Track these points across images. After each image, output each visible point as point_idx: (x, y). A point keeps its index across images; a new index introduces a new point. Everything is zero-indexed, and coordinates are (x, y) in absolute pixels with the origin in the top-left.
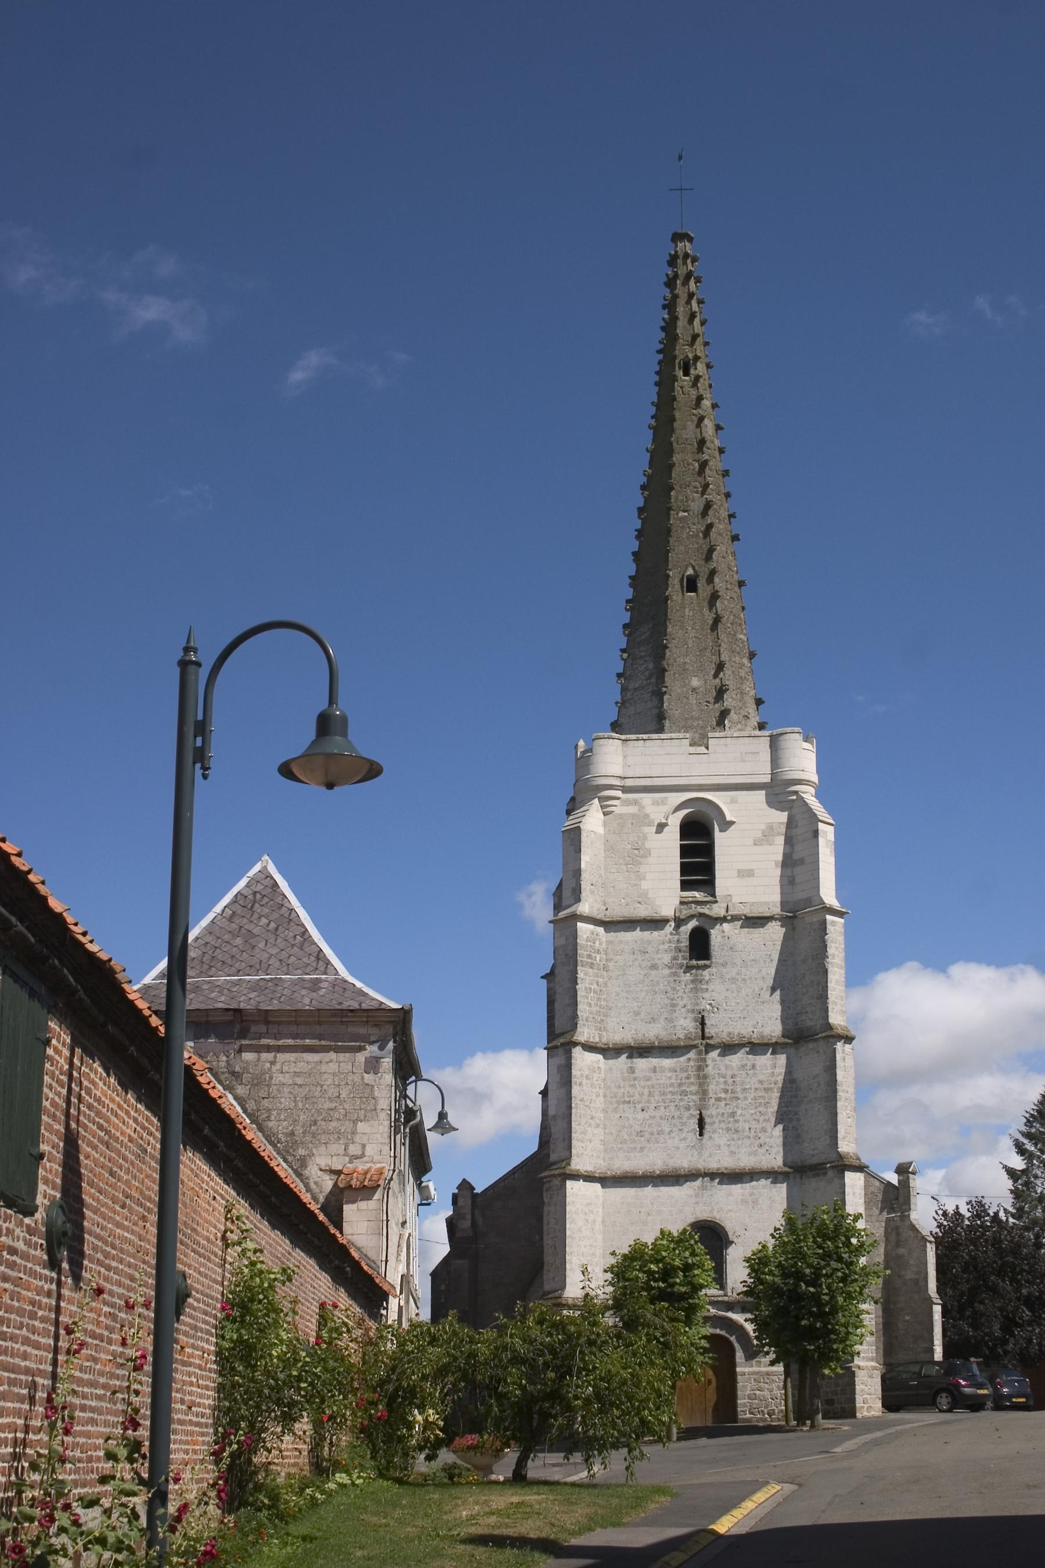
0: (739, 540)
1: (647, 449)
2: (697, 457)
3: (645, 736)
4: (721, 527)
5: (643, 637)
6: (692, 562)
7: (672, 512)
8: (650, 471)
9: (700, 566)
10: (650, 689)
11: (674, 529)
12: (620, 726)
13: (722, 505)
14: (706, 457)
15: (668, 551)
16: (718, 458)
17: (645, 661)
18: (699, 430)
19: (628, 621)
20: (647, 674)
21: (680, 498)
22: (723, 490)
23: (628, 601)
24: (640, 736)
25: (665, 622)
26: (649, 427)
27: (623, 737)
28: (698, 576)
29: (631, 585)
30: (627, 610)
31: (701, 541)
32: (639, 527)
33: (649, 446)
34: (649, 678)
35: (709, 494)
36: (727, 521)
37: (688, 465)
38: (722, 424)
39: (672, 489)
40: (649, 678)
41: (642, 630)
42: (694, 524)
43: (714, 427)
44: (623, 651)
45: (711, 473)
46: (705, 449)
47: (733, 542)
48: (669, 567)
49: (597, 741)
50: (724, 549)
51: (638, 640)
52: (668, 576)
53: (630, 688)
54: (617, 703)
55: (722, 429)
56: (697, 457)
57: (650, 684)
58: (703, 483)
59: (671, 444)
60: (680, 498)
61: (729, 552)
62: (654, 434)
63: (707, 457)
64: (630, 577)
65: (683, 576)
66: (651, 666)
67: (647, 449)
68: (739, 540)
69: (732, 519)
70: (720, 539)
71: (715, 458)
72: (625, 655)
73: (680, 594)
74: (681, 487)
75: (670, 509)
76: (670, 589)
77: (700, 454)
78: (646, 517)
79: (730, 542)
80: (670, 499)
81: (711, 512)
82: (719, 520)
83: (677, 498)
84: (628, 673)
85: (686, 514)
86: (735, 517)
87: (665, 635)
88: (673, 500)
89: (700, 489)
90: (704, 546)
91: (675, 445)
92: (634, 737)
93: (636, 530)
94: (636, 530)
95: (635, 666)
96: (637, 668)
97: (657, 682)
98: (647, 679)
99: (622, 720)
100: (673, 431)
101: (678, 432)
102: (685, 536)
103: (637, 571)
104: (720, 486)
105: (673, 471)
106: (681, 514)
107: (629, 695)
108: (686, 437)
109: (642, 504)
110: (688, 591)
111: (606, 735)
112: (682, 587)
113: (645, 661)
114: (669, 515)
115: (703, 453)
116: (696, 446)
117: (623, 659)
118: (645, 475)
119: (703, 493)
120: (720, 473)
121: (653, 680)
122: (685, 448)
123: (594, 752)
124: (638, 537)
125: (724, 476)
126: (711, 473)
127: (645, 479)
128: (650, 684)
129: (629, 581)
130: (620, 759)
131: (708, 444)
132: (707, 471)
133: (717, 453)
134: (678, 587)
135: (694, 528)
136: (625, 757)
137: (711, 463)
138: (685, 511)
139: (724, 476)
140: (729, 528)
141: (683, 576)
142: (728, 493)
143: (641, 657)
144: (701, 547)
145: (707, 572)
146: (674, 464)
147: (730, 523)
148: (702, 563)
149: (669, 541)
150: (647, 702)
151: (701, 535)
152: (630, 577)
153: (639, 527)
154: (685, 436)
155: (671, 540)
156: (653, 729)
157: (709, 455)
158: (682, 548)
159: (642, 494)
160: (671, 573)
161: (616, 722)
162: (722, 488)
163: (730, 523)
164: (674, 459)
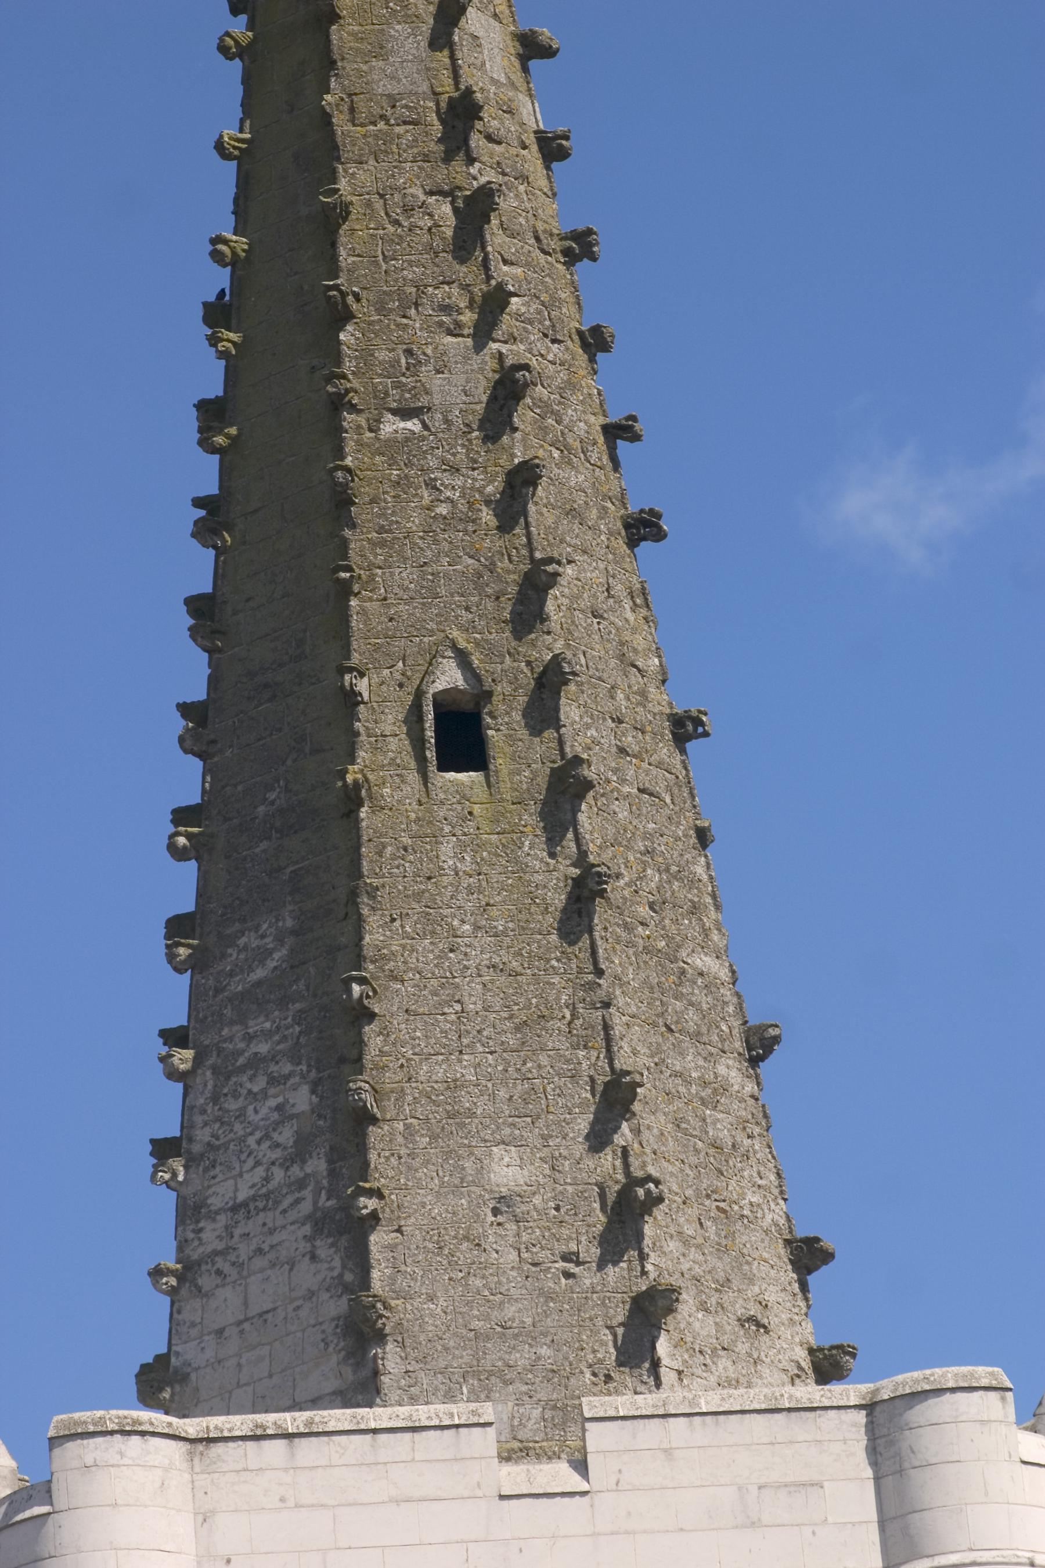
0: (659, 535)
1: (220, 146)
2: (441, 175)
3: (292, 1420)
4: (577, 478)
5: (259, 974)
6: (455, 634)
7: (349, 419)
8: (241, 243)
9: (491, 652)
10: (306, 1207)
11: (363, 492)
12: (181, 1378)
13: (572, 385)
14: (483, 175)
15: (345, 590)
16: (543, 183)
17: (273, 1081)
18: (443, 56)
19: (188, 905)
20: (286, 1135)
21: (382, 355)
22: (572, 320)
23: (182, 816)
24: (270, 1420)
25: (353, 895)
26: (223, 49)
27: (191, 1426)
28: (489, 694)
29: (187, 744)
30: (178, 854)
31: (491, 543)
32: (211, 487)
33: (229, 133)
34: (300, 1153)
35: (512, 339)
36: (599, 453)
37: (408, 210)
38: (545, 34)
39: (344, 316)
40: (300, 1153)
41: (250, 940)
42: (455, 470)
43: (514, 48)
44: (174, 1037)
45: (511, 247)
46: (476, 141)
47: (632, 543)
48: (356, 659)
49: (72, 1447)
50: (594, 575)
51: (237, 987)
52: (351, 700)
53: (216, 1203)
54: (157, 1273)
55: (548, 52)
56: (441, 175)
57: (301, 1184)
58: (479, 289)
59: (326, 119)
60: (382, 355)
61: (619, 589)
62: (247, 80)
63: (490, 176)
64: (185, 709)
65: (419, 694)
66: (302, 1099)
67: (220, 146)
68: (659, 535)
69: (623, 446)
70: (573, 534)
71: (524, 178)
72: (183, 1058)
73: (413, 777)
74: (381, 309)
75: (339, 403)
76: (363, 755)
77: (458, 165)
78: (234, 440)
79: (620, 545)
80: (337, 359)
81: (524, 417)
82: (565, 448)
83: (366, 354)
84: (203, 1135)
85: (413, 425)
86: (636, 438)
87: (358, 960)
88: (348, 366)
89: (468, 317)
90: (502, 564)
91: (340, 121)
92: (239, 1423)
93: (198, 503)
94: (198, 503)
95: (232, 1105)
96: (241, 1114)
97: (333, 1173)
98: (286, 1164)
99: (189, 1352)
100: (328, 64)
101: (348, 66)
102: (415, 521)
103: (214, 682)
104: (554, 303)
105: (343, 238)
106: (392, 426)
107: (211, 1235)
108: (392, 88)
109: (215, 389)
110: (443, 767)
111: (113, 1417)
112: (418, 743)
113: (273, 1081)
114: (337, 431)
115: (471, 160)
116: (437, 128)
117: (173, 1074)
118: (217, 256)
119: (483, 334)
120: (554, 244)
121: (317, 1165)
122: (388, 138)
123: (60, 1498)
124: (204, 532)
125: (571, 258)
126: (511, 247)
127: (221, 278)
128: (301, 1184)
129: (179, 724)
130: (184, 1525)
131: (491, 119)
132: (496, 239)
133: (532, 160)
134: (399, 745)
135: (453, 486)
136: (205, 1518)
137: (506, 203)
138: (405, 413)
139: (571, 258)
140: (613, 484)
141: (419, 694)
142: (597, 330)
143: (256, 1062)
144: (491, 568)
145: (527, 679)
146: (344, 211)
147: (616, 465)
148: (503, 637)
149: (345, 543)
150: (292, 1264)
151: (487, 516)
152: (185, 709)
153: (211, 487)
154: (384, 87)
155: (357, 542)
156: (332, 1384)
157: (499, 167)
158: (405, 575)
159: (213, 341)
160: (362, 686)
161: (162, 1360)
162: (568, 310)
163: (616, 465)
164: (343, 185)
